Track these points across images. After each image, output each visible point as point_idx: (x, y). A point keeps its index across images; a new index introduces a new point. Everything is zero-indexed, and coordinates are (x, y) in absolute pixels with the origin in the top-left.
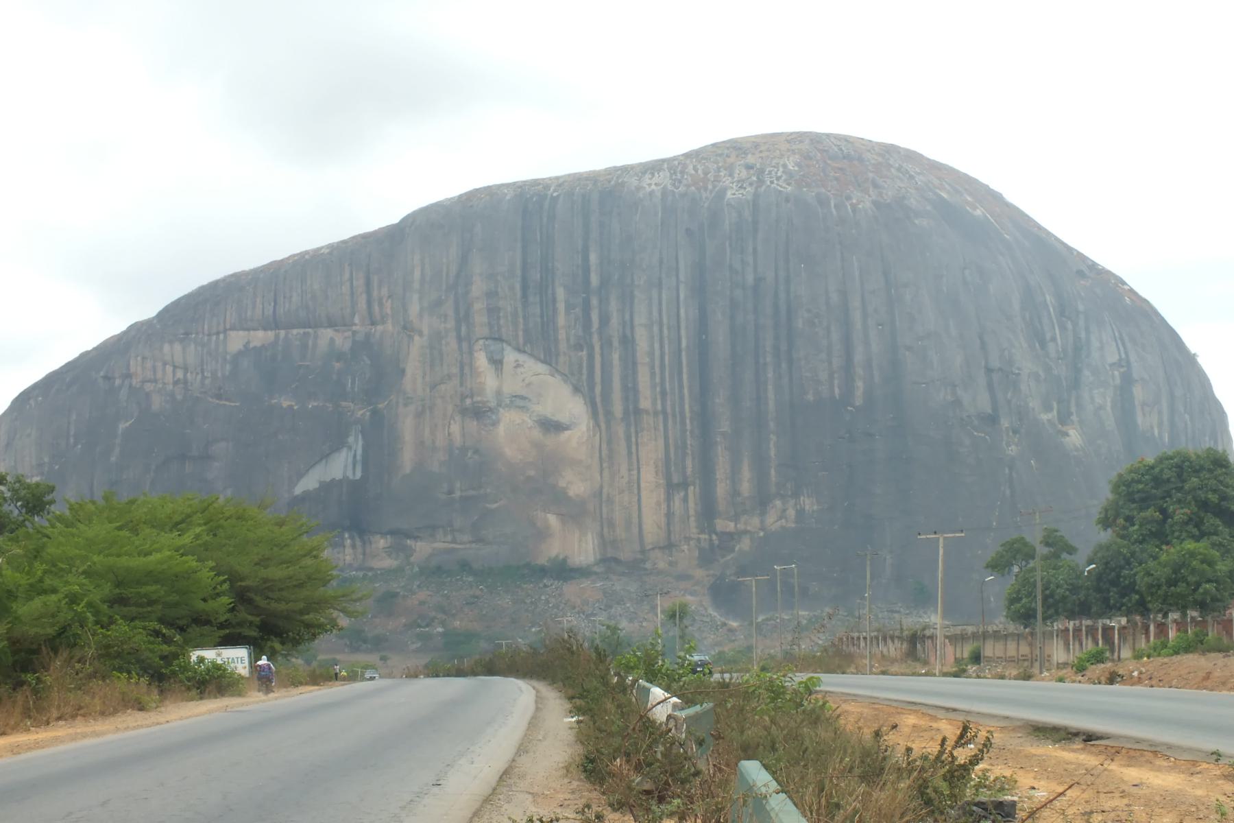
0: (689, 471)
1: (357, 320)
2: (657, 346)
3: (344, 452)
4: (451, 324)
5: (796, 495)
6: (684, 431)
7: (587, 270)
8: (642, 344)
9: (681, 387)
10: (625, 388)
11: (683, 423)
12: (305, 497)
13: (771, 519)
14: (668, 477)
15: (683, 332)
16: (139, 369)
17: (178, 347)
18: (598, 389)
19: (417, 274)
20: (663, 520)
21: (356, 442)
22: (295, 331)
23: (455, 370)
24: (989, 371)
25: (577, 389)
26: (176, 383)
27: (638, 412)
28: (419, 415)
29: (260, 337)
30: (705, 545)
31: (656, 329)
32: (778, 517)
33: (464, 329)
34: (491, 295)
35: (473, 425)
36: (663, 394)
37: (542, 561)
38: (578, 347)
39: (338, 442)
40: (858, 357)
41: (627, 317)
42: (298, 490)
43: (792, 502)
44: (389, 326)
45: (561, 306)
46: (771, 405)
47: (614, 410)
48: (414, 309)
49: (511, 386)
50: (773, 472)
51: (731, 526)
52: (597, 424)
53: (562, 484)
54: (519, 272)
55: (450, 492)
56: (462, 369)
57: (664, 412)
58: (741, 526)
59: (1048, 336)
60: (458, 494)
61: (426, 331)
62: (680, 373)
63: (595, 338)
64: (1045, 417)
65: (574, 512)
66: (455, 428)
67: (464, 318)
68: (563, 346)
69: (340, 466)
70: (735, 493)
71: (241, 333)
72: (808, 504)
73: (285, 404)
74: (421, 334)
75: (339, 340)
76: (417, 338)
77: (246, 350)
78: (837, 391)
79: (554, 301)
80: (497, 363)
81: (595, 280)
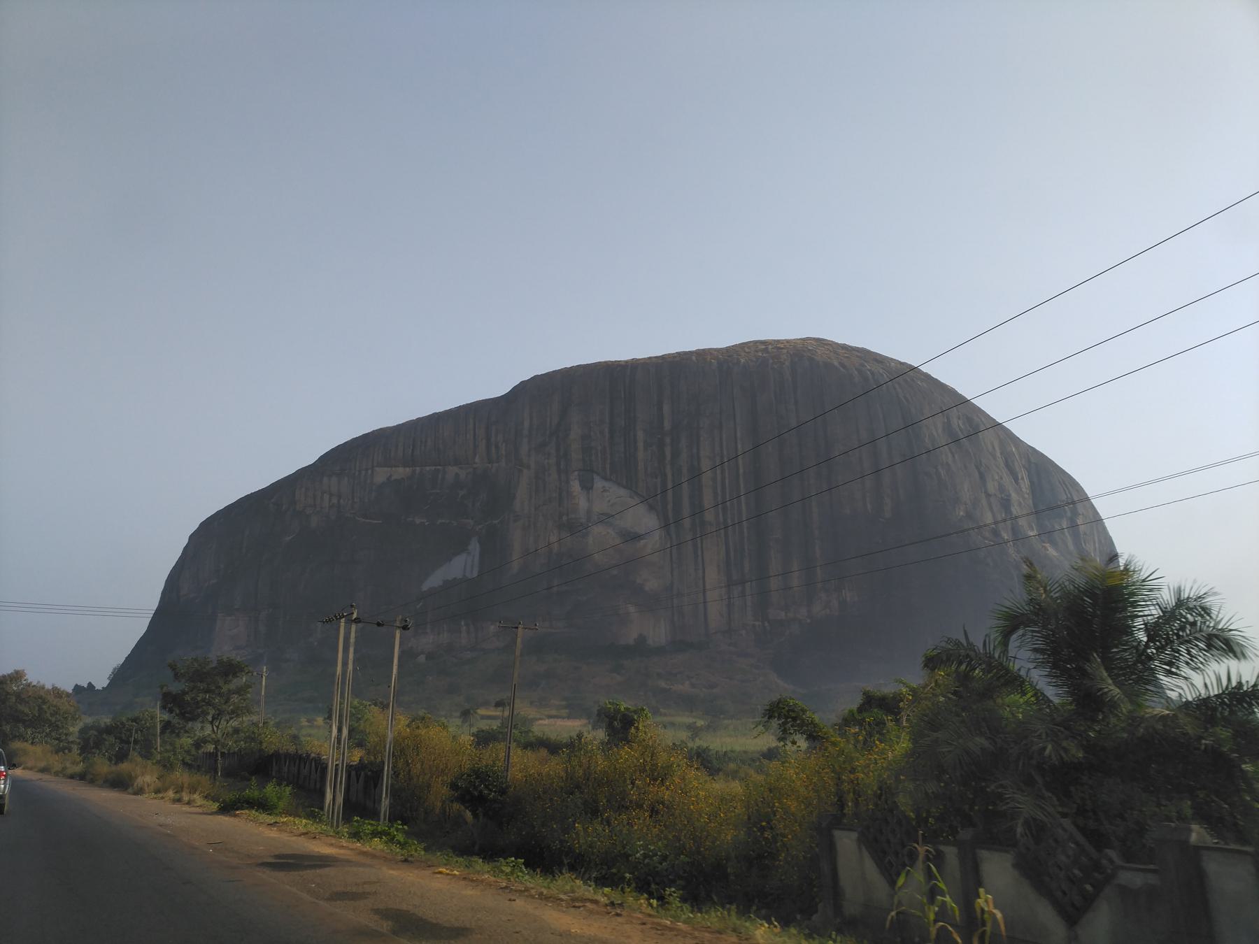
1: (477, 460)
3: (463, 557)
18: (670, 506)
19: (527, 424)
21: (475, 547)
29: (401, 472)
42: (425, 587)
45: (641, 445)
66: (553, 539)
69: (461, 566)
73: (418, 521)
74: (528, 467)
76: (525, 471)
78: (869, 506)
81: (667, 425)
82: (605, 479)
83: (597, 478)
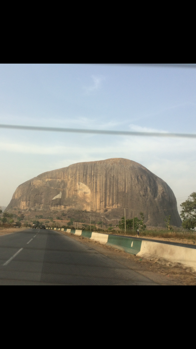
0: (103, 200)
4: (74, 179)
5: (117, 204)
6: (103, 195)
7: (92, 173)
8: (98, 183)
9: (103, 188)
10: (95, 188)
11: (103, 194)
12: (54, 200)
13: (114, 207)
14: (100, 200)
17: (39, 180)
18: (92, 188)
19: (70, 173)
20: (99, 206)
21: (61, 193)
23: (74, 185)
24: (144, 189)
25: (89, 188)
27: (97, 192)
28: (69, 190)
29: (50, 180)
30: (105, 210)
32: (115, 207)
35: (76, 192)
36: (100, 189)
37: (83, 210)
38: (90, 183)
39: (58, 193)
40: (127, 186)
42: (53, 199)
44: (66, 179)
45: (88, 178)
46: (115, 192)
47: (94, 191)
48: (69, 177)
49: (81, 188)
50: (114, 201)
51: (108, 207)
52: (91, 193)
53: (86, 200)
54: (83, 173)
55: (72, 200)
58: (110, 208)
60: (73, 201)
62: (103, 187)
63: (92, 182)
65: (88, 204)
66: (73, 192)
67: (76, 179)
68: (88, 183)
69: (59, 196)
70: (109, 203)
72: (119, 205)
77: (48, 181)
80: (79, 184)
82: (82, 183)
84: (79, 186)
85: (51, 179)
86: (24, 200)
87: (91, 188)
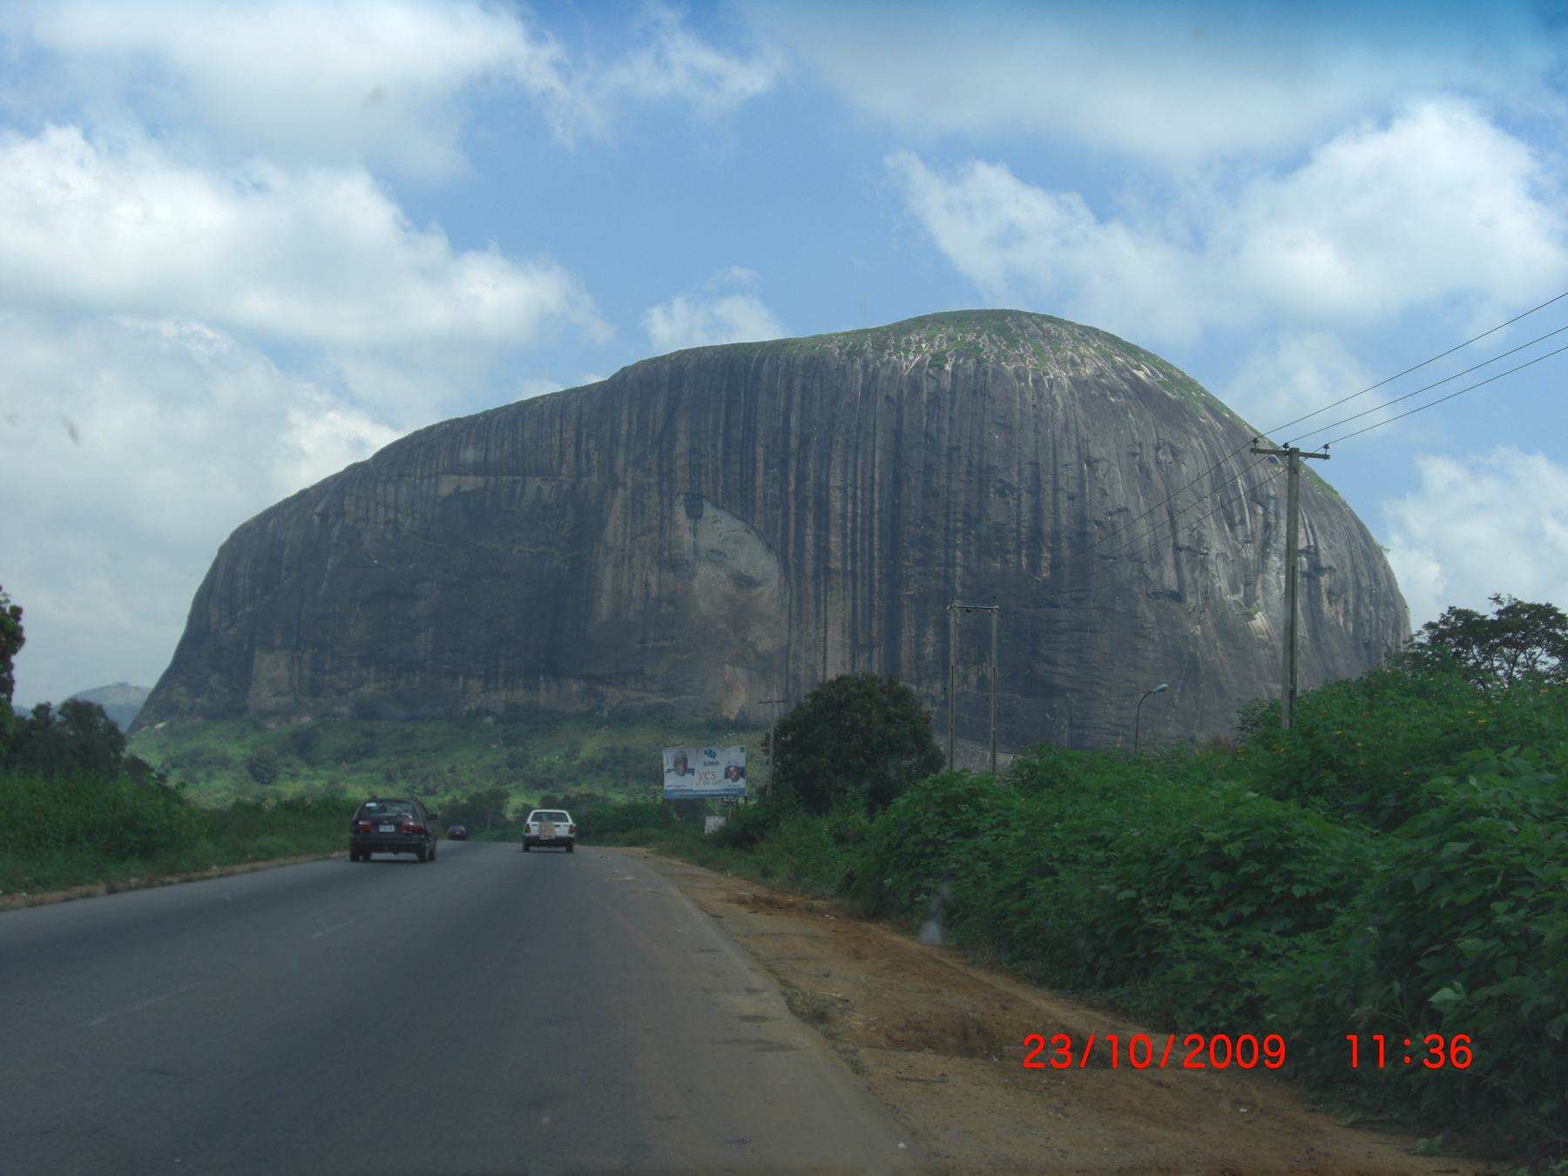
1: (564, 471)
2: (850, 507)
4: (654, 479)
8: (837, 505)
11: (871, 585)
15: (876, 495)
16: (353, 509)
17: (391, 488)
18: (791, 549)
19: (624, 428)
22: (504, 478)
23: (655, 523)
24: (1177, 549)
25: (770, 547)
26: (387, 522)
27: (828, 570)
29: (470, 483)
31: (850, 490)
33: (666, 484)
34: (693, 451)
36: (854, 555)
40: (1048, 528)
41: (823, 478)
43: (975, 668)
45: (760, 466)
48: (620, 461)
49: (707, 540)
55: (643, 641)
56: (662, 521)
57: (854, 573)
58: (923, 690)
59: (1237, 519)
60: (650, 644)
61: (629, 483)
62: (872, 535)
63: (791, 497)
64: (1230, 598)
68: (759, 504)
71: (453, 478)
74: (624, 485)
75: (546, 489)
76: (620, 490)
79: (754, 460)
81: (794, 443)
82: (719, 508)
83: (707, 505)
84: (695, 532)
85: (481, 481)
86: (278, 642)
87: (785, 546)
